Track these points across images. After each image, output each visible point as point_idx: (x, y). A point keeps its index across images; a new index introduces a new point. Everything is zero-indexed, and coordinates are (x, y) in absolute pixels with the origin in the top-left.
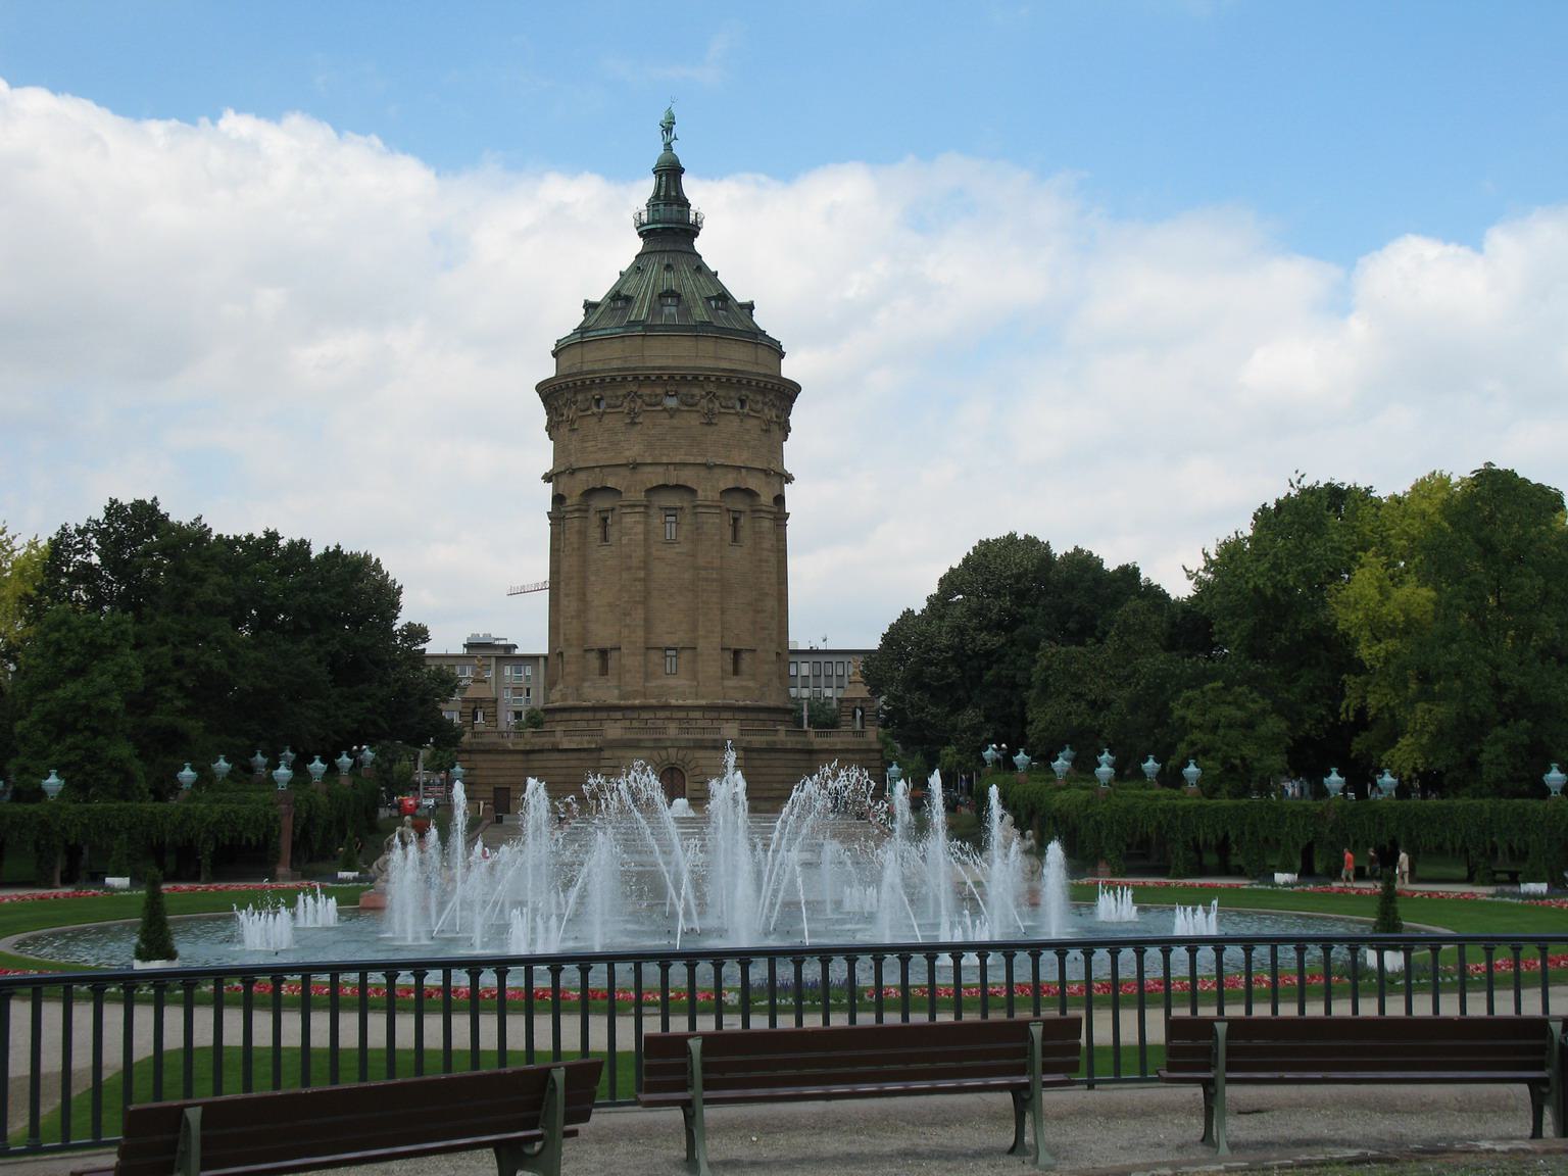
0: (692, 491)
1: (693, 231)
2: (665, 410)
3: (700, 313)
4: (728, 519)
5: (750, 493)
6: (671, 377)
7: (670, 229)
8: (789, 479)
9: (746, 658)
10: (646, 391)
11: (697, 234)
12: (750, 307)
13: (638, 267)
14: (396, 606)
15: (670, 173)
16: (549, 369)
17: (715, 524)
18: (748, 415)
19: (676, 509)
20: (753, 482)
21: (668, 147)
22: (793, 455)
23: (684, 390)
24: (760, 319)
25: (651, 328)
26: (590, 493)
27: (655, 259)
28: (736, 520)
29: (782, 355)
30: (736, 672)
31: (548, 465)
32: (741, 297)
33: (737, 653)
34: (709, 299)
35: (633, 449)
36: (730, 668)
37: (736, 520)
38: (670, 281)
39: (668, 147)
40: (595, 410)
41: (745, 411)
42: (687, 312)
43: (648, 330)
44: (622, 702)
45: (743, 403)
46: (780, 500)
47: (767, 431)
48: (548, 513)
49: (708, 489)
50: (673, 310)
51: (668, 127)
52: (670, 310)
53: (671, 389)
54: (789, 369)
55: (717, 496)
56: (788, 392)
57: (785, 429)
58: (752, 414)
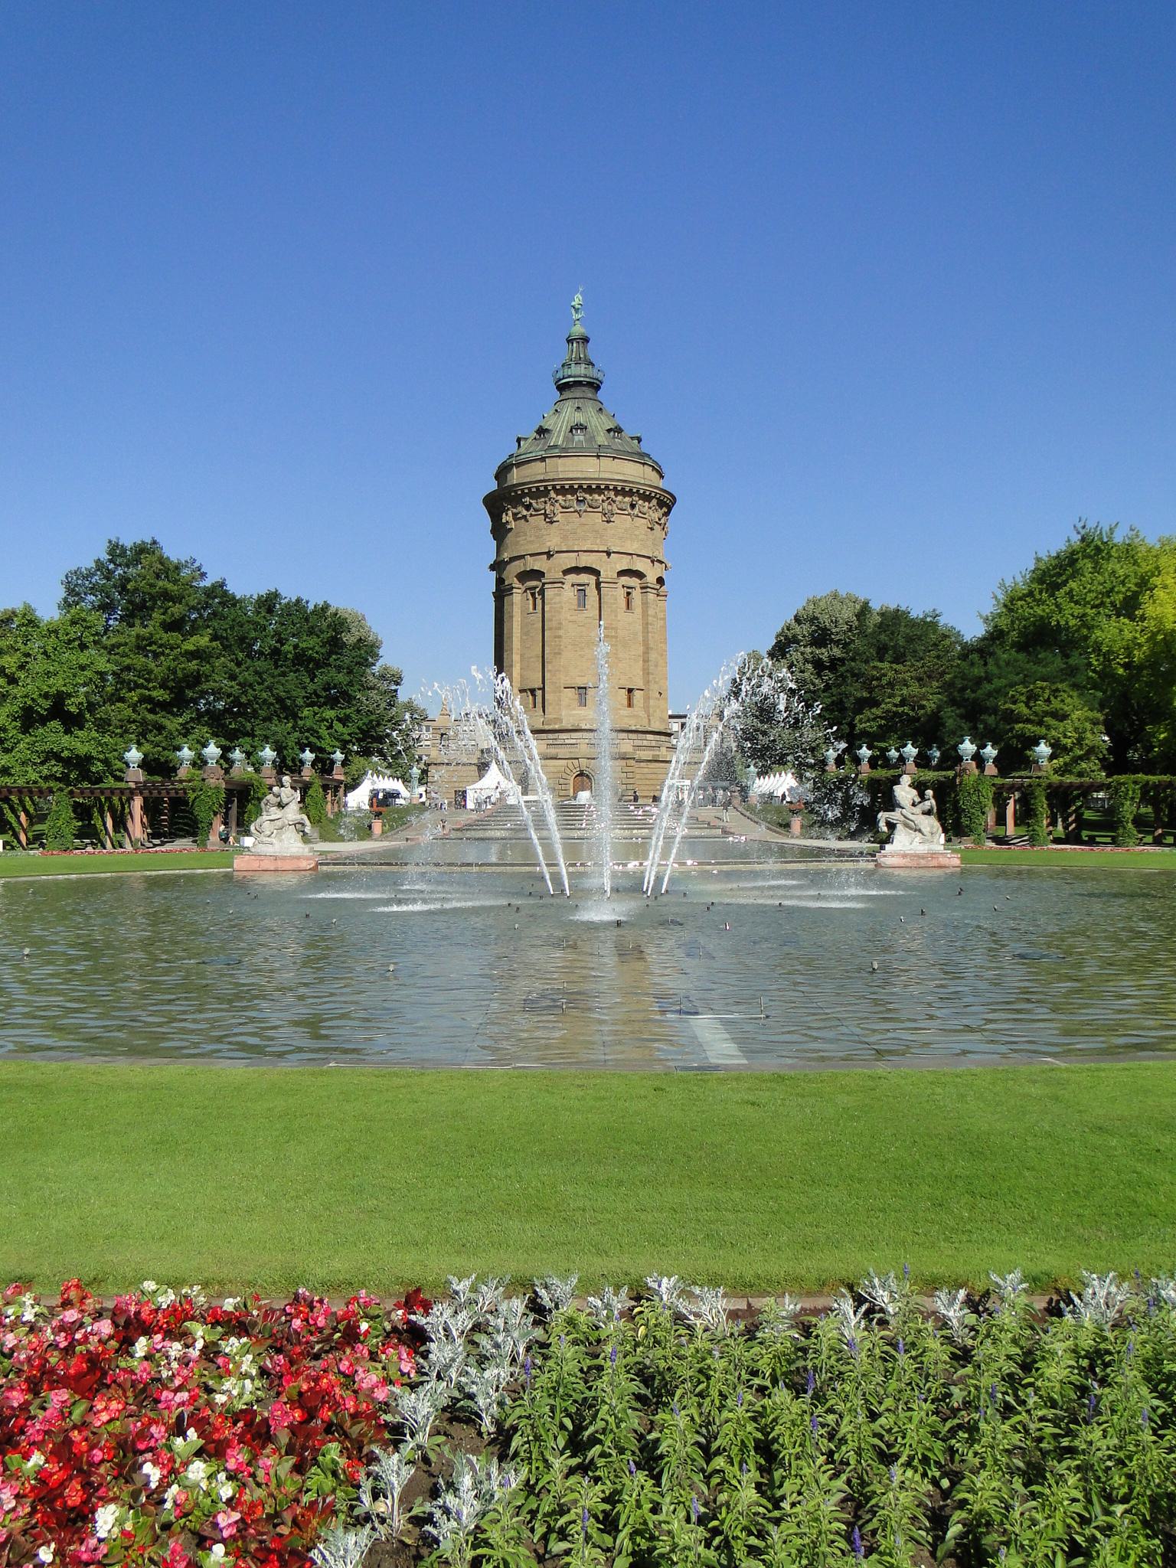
0: (596, 573)
1: (595, 386)
3: (602, 439)
4: (622, 592)
5: (639, 575)
6: (580, 486)
9: (636, 693)
11: (598, 388)
12: (639, 440)
14: (376, 656)
16: (493, 486)
17: (615, 595)
20: (640, 565)
23: (587, 496)
25: (565, 450)
26: (524, 576)
27: (569, 403)
28: (628, 594)
30: (630, 705)
31: (492, 558)
33: (630, 691)
34: (609, 431)
35: (552, 539)
36: (626, 702)
37: (628, 594)
38: (579, 418)
40: (525, 512)
42: (592, 438)
43: (564, 453)
44: (547, 727)
45: (633, 506)
49: (608, 569)
50: (582, 438)
52: (579, 437)
53: (581, 495)
56: (666, 503)
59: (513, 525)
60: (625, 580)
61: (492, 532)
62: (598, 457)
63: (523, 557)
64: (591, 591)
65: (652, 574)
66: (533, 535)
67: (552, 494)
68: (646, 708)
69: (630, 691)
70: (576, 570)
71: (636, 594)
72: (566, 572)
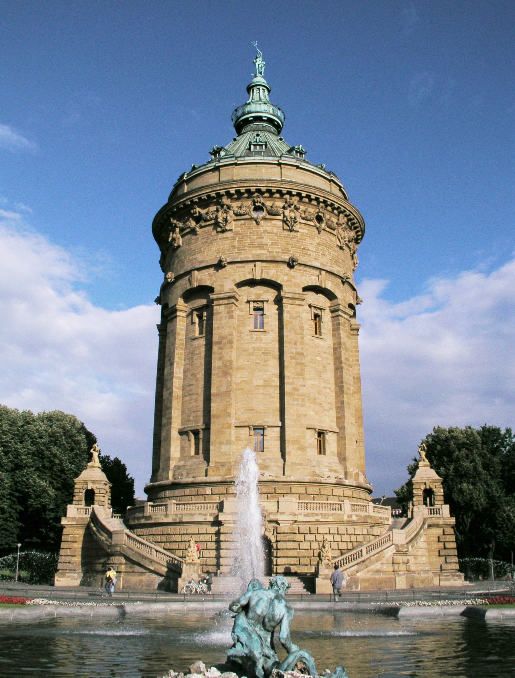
0: (277, 287)
2: (251, 218)
5: (330, 295)
9: (331, 439)
10: (235, 205)
18: (324, 230)
19: (262, 302)
23: (268, 204)
28: (316, 316)
33: (321, 434)
41: (323, 225)
47: (341, 248)
48: (157, 325)
49: (293, 281)
55: (300, 291)
58: (327, 229)
59: (180, 241)
60: (312, 297)
61: (160, 262)
62: (279, 164)
63: (189, 273)
64: (271, 310)
65: (344, 296)
66: (202, 248)
67: (225, 201)
68: (342, 458)
69: (321, 434)
70: (252, 283)
71: (327, 317)
72: (240, 285)
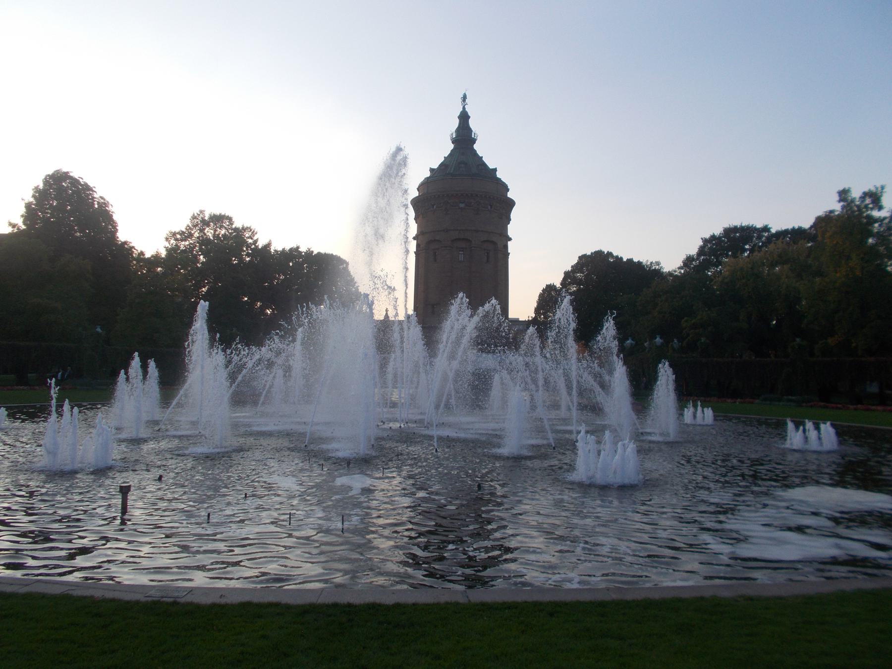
1: (474, 141)
7: (464, 138)
8: (510, 239)
12: (495, 170)
13: (450, 155)
15: (464, 117)
21: (464, 108)
22: (512, 230)
24: (499, 175)
29: (508, 190)
32: (491, 166)
39: (464, 108)
46: (506, 247)
51: (464, 98)
54: (510, 195)
57: (509, 220)
